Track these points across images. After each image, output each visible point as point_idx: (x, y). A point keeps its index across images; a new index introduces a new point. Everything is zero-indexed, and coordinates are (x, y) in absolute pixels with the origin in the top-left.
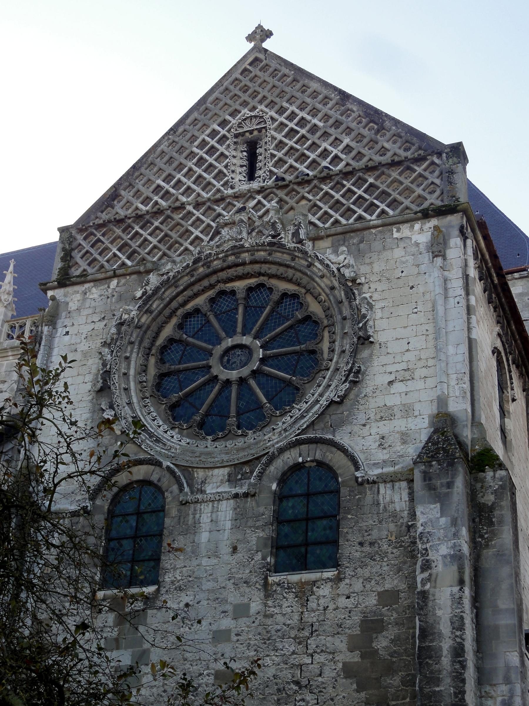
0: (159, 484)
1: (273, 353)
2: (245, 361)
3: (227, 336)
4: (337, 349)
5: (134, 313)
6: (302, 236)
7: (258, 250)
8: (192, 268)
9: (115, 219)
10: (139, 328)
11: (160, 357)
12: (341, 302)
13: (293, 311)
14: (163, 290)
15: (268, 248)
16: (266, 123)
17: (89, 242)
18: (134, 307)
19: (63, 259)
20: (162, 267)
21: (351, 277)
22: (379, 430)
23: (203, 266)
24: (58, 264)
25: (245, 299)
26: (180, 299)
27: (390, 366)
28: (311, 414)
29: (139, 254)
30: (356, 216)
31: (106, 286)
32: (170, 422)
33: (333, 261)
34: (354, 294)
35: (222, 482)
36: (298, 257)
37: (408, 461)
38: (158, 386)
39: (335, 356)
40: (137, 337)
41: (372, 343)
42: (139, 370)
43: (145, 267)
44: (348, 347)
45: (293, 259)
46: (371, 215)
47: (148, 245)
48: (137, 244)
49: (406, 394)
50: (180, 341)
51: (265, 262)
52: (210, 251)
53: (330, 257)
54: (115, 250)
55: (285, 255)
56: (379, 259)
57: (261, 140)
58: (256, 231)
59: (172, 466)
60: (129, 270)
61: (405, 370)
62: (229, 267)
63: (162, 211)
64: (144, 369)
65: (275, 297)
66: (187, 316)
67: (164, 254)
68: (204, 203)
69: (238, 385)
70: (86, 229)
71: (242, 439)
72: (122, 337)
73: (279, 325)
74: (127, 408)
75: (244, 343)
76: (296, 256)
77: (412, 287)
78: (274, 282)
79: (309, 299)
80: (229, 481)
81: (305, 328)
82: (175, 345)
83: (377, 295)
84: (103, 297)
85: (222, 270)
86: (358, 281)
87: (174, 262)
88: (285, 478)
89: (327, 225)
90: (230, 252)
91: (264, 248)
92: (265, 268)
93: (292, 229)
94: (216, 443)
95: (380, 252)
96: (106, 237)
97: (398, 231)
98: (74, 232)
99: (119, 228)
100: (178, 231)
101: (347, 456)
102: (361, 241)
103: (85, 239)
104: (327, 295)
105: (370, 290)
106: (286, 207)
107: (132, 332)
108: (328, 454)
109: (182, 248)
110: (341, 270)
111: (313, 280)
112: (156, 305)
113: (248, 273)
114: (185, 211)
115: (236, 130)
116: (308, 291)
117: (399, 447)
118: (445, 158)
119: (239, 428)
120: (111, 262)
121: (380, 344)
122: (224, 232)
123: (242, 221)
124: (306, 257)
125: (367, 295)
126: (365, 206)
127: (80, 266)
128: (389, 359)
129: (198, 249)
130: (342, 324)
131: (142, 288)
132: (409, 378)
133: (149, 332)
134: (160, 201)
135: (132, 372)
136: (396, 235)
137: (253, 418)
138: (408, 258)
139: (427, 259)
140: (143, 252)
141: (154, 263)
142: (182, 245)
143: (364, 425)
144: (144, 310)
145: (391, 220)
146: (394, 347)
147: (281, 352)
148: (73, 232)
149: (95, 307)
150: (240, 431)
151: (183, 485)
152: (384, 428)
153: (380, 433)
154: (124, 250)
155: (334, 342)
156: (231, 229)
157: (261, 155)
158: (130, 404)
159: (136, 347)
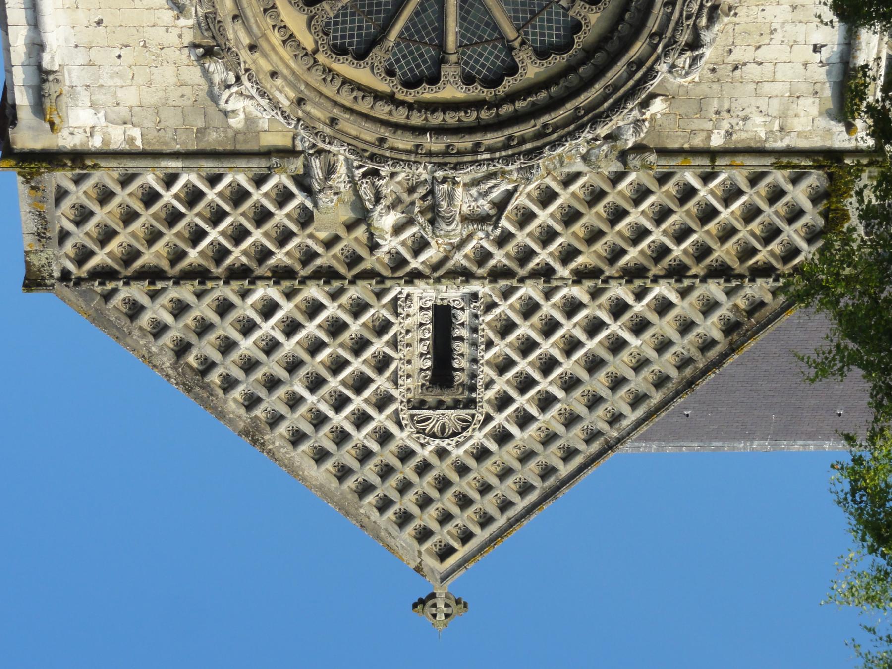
14: (606, 105)
15: (388, 154)
16: (412, 416)
31: (735, 137)
36: (324, 124)
45: (333, 121)
51: (396, 127)
55: (354, 133)
57: (423, 385)
68: (534, 274)
77: (99, 23)
90: (466, 159)
91: (394, 155)
97: (132, 140)
103: (795, 252)
110: (234, 80)
113: (433, 113)
115: (473, 416)
118: (54, 267)
134: (630, 299)
138: (110, 83)
139: (75, 74)
157: (422, 355)
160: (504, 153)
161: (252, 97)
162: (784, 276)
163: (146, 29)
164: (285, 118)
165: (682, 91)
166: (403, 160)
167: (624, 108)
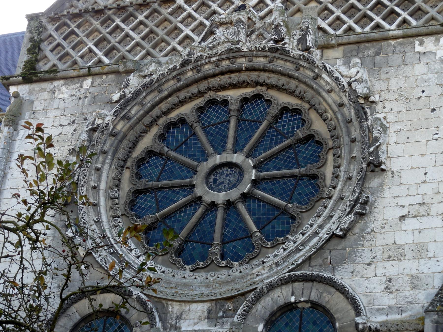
0: (127, 316)
1: (268, 175)
2: (234, 182)
3: (215, 152)
4: (342, 174)
5: (109, 118)
6: (310, 42)
7: (257, 56)
8: (180, 71)
9: (93, 9)
10: (114, 136)
11: (135, 171)
12: (350, 122)
13: (293, 128)
14: (144, 94)
15: (269, 54)
17: (62, 34)
18: (110, 112)
19: (30, 51)
20: (145, 68)
21: (364, 94)
22: (385, 271)
23: (192, 69)
24: (24, 57)
25: (238, 110)
26: (164, 106)
27: (403, 198)
28: (308, 248)
29: (119, 51)
30: (372, 24)
31: (79, 85)
32: (144, 246)
33: (343, 74)
34: (365, 113)
35: (200, 318)
36: (303, 66)
37: (417, 309)
38: (132, 204)
39: (340, 183)
40: (111, 146)
41: (383, 170)
42: (111, 184)
43: (125, 66)
44: (355, 173)
46: (390, 24)
47: (130, 42)
48: (118, 39)
49: (420, 232)
50: (160, 154)
51: (264, 70)
52: (201, 53)
53: (341, 69)
54: (91, 45)
55: (288, 64)
56: (397, 75)
58: (256, 33)
59: (143, 296)
60: (107, 69)
61: (420, 204)
62: (222, 73)
63: (148, 4)
64: (117, 183)
65: (274, 110)
66: (170, 125)
67: (148, 53)
69: (225, 209)
70: (59, 19)
71: (225, 272)
72: (94, 145)
73: (276, 144)
74: (94, 227)
75: (234, 161)
76: (301, 66)
77: (433, 110)
78: (273, 94)
79: (313, 115)
80: (208, 318)
81: (307, 149)
82: (154, 158)
83: (392, 117)
84: (74, 98)
85: (214, 76)
86: (372, 99)
87: (159, 63)
88: (274, 318)
89: (339, 32)
90: (225, 56)
91: (265, 53)
92: (263, 77)
93: (298, 34)
94: (195, 274)
95: (399, 67)
96: (81, 29)
97: (421, 44)
98: (44, 21)
99: (97, 19)
100: (166, 28)
101: (348, 299)
102: (378, 54)
103: (57, 29)
104: (335, 113)
105: (385, 110)
106: (293, 9)
107: (106, 140)
108: (325, 294)
109: (169, 48)
110: (353, 85)
111: (319, 94)
112: (135, 111)
113: (244, 82)
114: (175, 6)
116: (312, 106)
117: (407, 292)
119: (223, 258)
120: (86, 58)
121: (393, 173)
122: (219, 32)
123: (240, 21)
124: (312, 67)
125: (381, 116)
126: (384, 13)
127: (49, 61)
128: (402, 191)
129: (188, 49)
130: (350, 146)
131: (120, 90)
132: (424, 213)
133: (125, 142)
135: (103, 186)
136: (418, 48)
137: (240, 248)
138: (430, 76)
140: (124, 49)
141: (136, 62)
142: (169, 44)
143: (369, 264)
144: (121, 116)
145: (414, 31)
146: (408, 177)
147: (277, 174)
148: (43, 21)
149: (64, 109)
150: (224, 262)
151: (155, 319)
152: (392, 269)
153: (387, 274)
154: (101, 45)
155: (339, 167)
156: (227, 29)
158: (98, 222)
159: (109, 157)
160: (203, 62)
161: (343, 76)
162: (65, 15)
163: (405, 110)
164: (325, 67)
165: (103, 106)
166: (260, 51)
167: (133, 94)
